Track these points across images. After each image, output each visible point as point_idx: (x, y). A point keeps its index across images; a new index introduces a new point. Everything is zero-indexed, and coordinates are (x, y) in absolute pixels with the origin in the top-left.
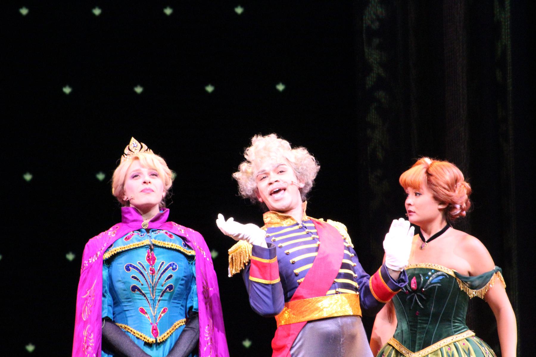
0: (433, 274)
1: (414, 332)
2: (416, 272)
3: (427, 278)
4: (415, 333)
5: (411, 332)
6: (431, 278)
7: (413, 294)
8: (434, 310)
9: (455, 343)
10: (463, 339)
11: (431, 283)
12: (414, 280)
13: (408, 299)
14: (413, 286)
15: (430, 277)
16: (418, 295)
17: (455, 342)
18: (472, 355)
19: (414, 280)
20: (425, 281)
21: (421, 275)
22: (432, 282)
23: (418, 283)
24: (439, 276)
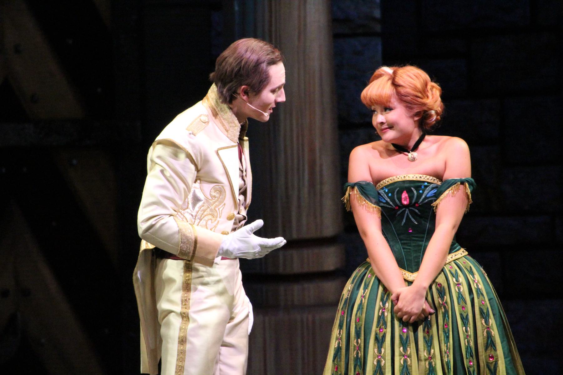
0: (426, 187)
1: (408, 250)
2: (407, 185)
3: (421, 192)
4: (409, 252)
5: (405, 250)
6: (426, 192)
7: (404, 209)
8: (430, 226)
9: (455, 262)
10: (462, 257)
11: (426, 198)
12: (405, 195)
13: (399, 215)
14: (405, 203)
15: (424, 191)
16: (409, 210)
17: (455, 260)
18: (475, 274)
19: (405, 195)
20: (419, 196)
21: (412, 188)
22: (428, 196)
23: (411, 198)
24: (433, 188)
